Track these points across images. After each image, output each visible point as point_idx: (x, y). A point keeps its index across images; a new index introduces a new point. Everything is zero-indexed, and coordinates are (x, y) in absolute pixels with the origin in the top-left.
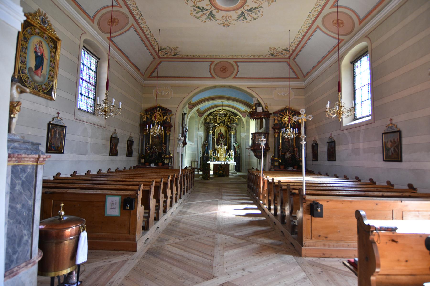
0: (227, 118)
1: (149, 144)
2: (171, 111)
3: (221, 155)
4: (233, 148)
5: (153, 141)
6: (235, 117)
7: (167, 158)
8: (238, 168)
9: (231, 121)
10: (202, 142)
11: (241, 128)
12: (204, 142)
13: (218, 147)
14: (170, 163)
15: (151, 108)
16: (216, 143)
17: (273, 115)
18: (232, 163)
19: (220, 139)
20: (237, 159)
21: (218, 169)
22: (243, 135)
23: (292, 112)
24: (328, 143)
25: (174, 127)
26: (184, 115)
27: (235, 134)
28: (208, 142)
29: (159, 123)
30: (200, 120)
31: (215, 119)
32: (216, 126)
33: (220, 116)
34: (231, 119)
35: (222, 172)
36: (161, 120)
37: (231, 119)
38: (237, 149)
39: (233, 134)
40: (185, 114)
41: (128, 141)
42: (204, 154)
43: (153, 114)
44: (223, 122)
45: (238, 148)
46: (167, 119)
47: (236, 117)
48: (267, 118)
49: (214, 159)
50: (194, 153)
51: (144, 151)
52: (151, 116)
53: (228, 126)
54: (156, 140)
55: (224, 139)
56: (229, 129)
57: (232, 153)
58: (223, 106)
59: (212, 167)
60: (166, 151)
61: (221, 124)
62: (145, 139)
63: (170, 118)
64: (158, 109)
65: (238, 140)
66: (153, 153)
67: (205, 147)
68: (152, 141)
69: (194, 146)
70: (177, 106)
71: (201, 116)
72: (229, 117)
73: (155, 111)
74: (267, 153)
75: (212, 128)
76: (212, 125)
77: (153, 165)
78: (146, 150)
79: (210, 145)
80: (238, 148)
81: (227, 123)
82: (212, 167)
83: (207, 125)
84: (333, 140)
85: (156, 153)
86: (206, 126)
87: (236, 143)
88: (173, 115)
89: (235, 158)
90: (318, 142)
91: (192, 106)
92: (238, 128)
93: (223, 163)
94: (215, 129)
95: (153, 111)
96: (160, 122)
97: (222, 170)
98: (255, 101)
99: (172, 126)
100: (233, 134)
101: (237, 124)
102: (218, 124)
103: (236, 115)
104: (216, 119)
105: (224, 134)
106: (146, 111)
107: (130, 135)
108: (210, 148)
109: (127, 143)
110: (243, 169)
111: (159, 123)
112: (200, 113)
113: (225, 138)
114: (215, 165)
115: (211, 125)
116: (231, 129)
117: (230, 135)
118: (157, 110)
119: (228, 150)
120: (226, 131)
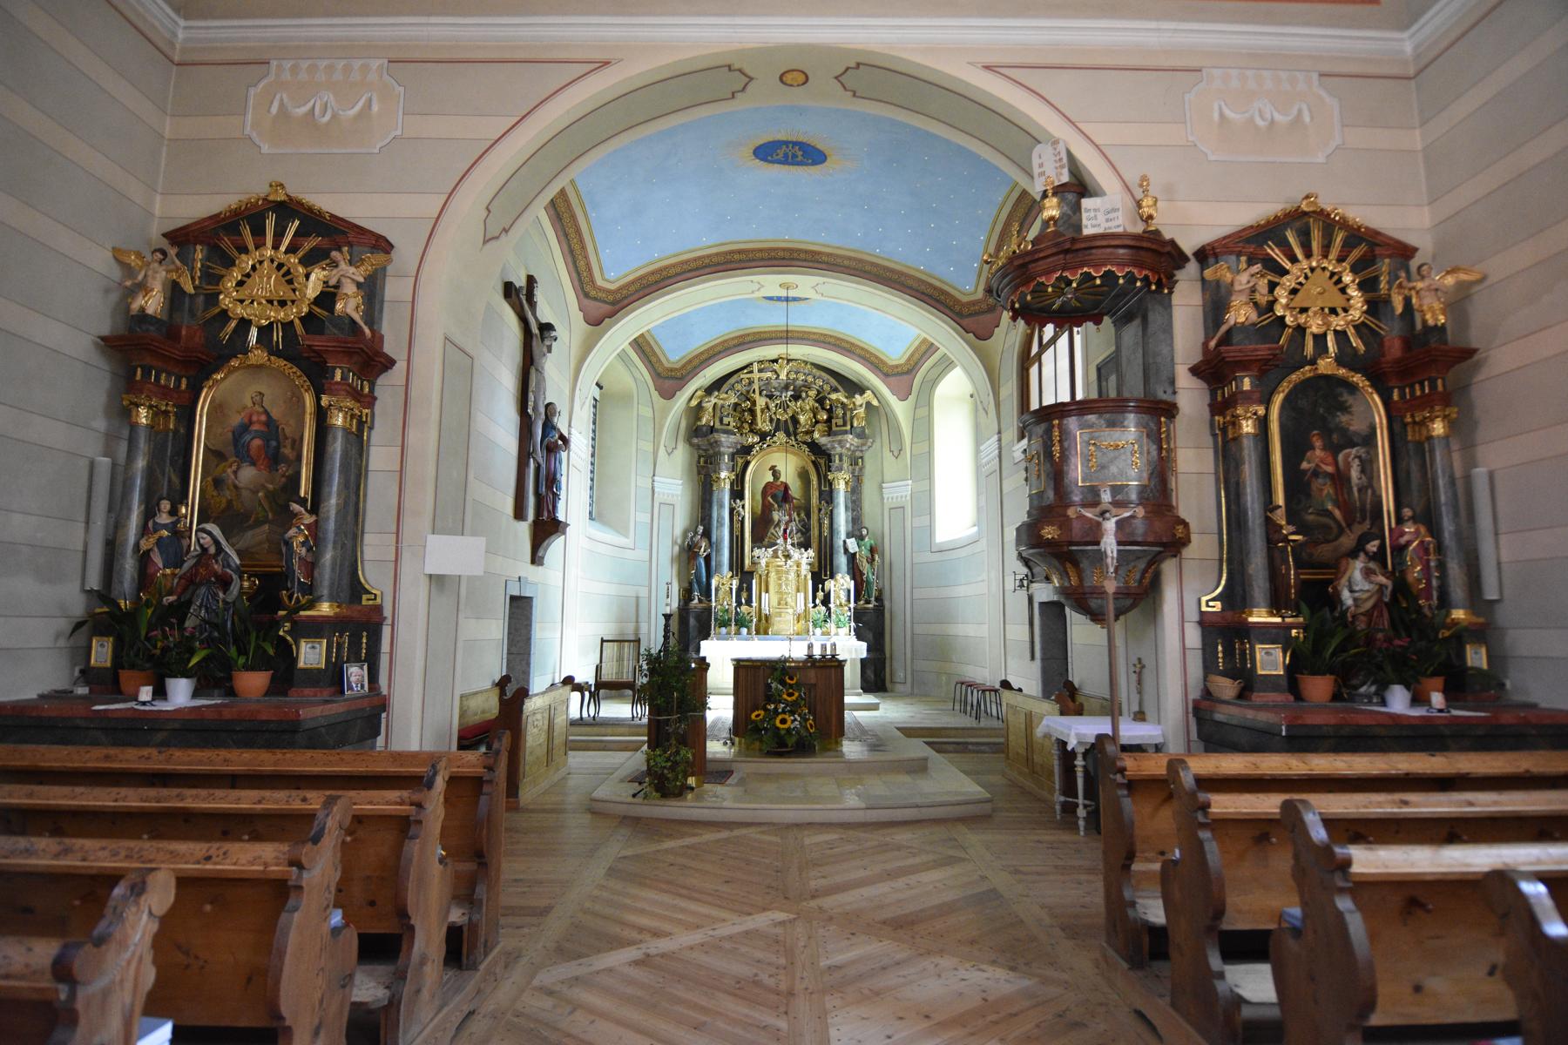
0: (810, 403)
3: (782, 602)
4: (842, 561)
5: (218, 483)
6: (850, 396)
7: (316, 629)
8: (876, 678)
9: (825, 417)
10: (678, 531)
11: (887, 455)
13: (764, 555)
14: (356, 674)
15: (214, 218)
16: (754, 541)
17: (1192, 267)
18: (851, 649)
19: (776, 516)
20: (872, 622)
21: (769, 699)
22: (899, 491)
23: (1348, 246)
25: (401, 366)
26: (536, 337)
28: (707, 534)
29: (277, 336)
31: (745, 413)
32: (751, 447)
33: (770, 397)
34: (830, 411)
35: (793, 722)
36: (292, 313)
37: (830, 411)
38: (865, 568)
39: (841, 487)
40: (546, 328)
42: (687, 595)
43: (230, 263)
44: (790, 427)
45: (871, 561)
46: (327, 298)
47: (859, 399)
48: (1160, 284)
49: (741, 622)
50: (630, 591)
51: (129, 565)
52: (212, 279)
53: (814, 447)
54: (248, 474)
55: (799, 513)
56: (821, 458)
57: (841, 585)
59: (720, 676)
60: (311, 567)
61: (781, 436)
62: (141, 463)
64: (270, 224)
65: (867, 521)
66: (191, 581)
67: (692, 558)
68: (215, 482)
69: (629, 554)
70: (433, 204)
71: (668, 394)
72: (820, 400)
73: (250, 241)
74: (1169, 567)
75: (732, 457)
76: (727, 443)
77: (181, 693)
78: (144, 559)
79: (719, 551)
80: (871, 561)
82: (720, 676)
83: (699, 434)
85: (225, 583)
86: (698, 447)
87: (860, 538)
89: (858, 616)
91: (604, 307)
92: (867, 456)
93: (798, 651)
94: (747, 464)
95: (226, 243)
96: (288, 326)
97: (790, 709)
98: (1050, 169)
99: (390, 363)
101: (861, 435)
102: (763, 436)
103: (854, 387)
104: (752, 412)
105: (795, 490)
106: (181, 238)
108: (719, 565)
110: (900, 675)
111: (277, 336)
112: (669, 380)
113: (798, 509)
114: (744, 669)
115: (723, 438)
116: (829, 458)
117: (828, 496)
118: (259, 232)
119: (822, 572)
120: (804, 476)
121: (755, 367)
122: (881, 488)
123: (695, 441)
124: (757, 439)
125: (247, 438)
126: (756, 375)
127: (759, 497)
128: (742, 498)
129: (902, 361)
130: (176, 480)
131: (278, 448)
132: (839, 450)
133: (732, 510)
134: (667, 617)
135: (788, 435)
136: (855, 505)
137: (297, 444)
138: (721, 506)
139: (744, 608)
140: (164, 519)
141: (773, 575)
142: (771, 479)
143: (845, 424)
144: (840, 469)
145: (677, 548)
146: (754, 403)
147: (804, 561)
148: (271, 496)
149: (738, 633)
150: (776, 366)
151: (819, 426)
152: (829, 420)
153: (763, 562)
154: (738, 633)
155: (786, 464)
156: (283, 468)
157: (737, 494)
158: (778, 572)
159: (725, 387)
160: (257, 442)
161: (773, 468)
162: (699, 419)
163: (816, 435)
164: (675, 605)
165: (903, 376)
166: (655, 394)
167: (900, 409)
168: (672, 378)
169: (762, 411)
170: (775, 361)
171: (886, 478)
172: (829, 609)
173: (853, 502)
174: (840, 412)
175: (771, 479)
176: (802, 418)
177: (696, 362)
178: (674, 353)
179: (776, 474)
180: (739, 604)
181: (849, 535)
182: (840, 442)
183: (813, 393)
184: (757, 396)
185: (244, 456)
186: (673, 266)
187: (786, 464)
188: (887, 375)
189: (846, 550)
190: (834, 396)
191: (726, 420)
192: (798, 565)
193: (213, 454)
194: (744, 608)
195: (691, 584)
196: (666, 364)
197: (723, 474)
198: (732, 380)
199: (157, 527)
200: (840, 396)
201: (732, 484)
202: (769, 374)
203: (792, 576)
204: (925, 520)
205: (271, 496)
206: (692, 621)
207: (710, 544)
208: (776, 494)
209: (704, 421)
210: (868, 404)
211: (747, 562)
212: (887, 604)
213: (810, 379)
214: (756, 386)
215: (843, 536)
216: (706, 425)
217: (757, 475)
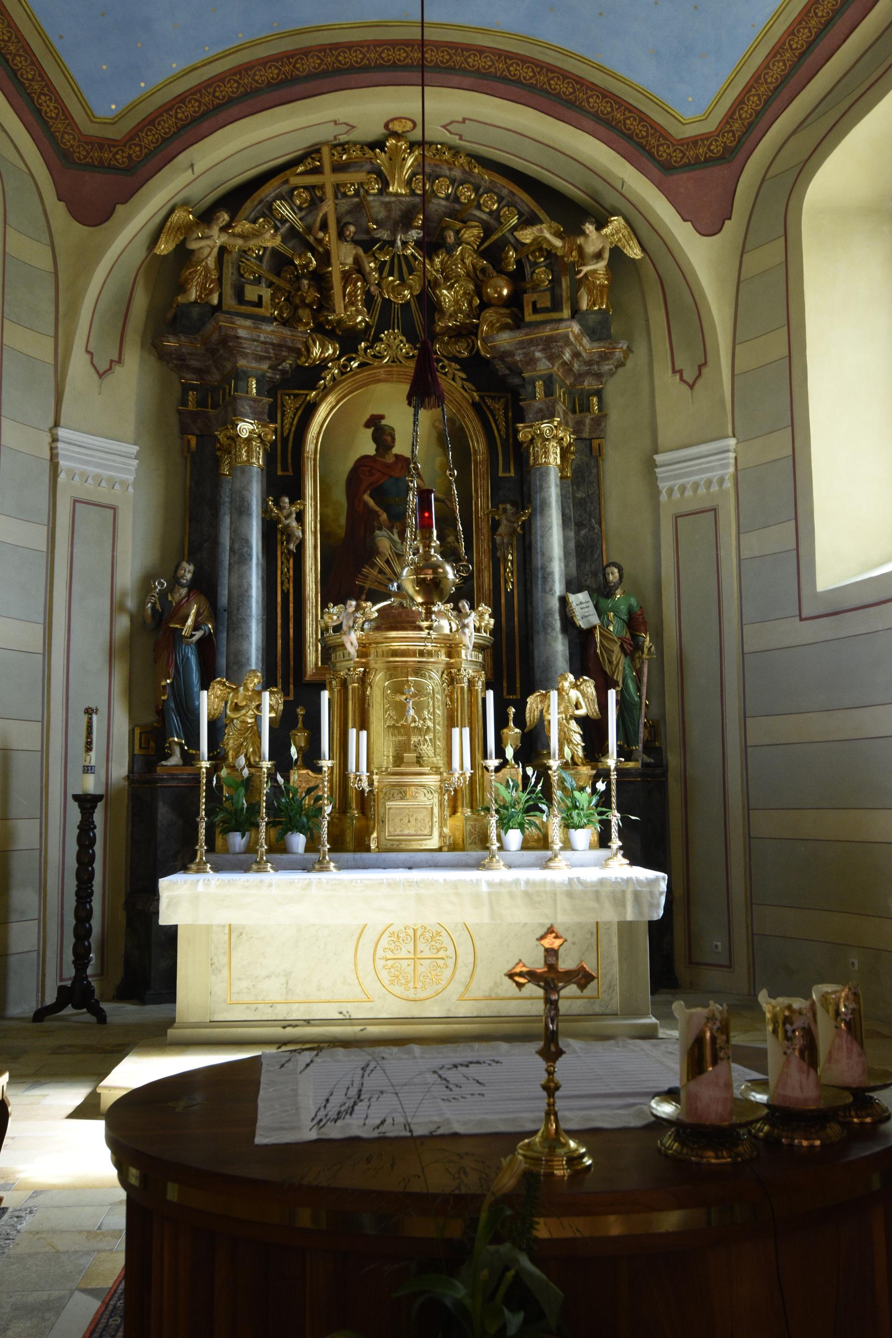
10: (128, 576)
12: (146, 583)
13: (353, 625)
22: (703, 466)
27: (584, 477)
28: (205, 585)
30: (86, 260)
31: (298, 281)
32: (322, 366)
33: (367, 244)
34: (518, 278)
37: (518, 278)
45: (632, 649)
47: (593, 239)
49: (289, 816)
72: (492, 253)
75: (270, 388)
76: (255, 338)
80: (632, 649)
87: (602, 593)
92: (613, 389)
94: (311, 409)
100: (554, 459)
102: (349, 339)
103: (573, 212)
104: (320, 280)
119: (513, 669)
121: (325, 150)
122: (651, 466)
123: (171, 343)
126: (328, 179)
127: (340, 494)
128: (297, 494)
129: (711, 125)
132: (544, 366)
134: (87, 803)
136: (585, 513)
138: (242, 510)
139: (299, 777)
141: (379, 680)
142: (369, 448)
143: (556, 306)
145: (123, 623)
146: (325, 258)
147: (469, 638)
149: (279, 847)
150: (381, 159)
151: (489, 314)
152: (514, 302)
153: (352, 640)
154: (279, 847)
157: (284, 482)
158: (393, 671)
159: (249, 206)
161: (375, 422)
162: (182, 288)
164: (120, 770)
166: (58, 211)
167: (702, 256)
170: (378, 144)
171: (665, 437)
172: (543, 772)
173: (580, 504)
174: (543, 275)
175: (369, 448)
176: (446, 295)
177: (168, 124)
180: (282, 762)
181: (572, 586)
183: (472, 234)
184: (330, 238)
188: (667, 167)
190: (527, 236)
191: (251, 293)
192: (452, 650)
194: (299, 777)
195: (161, 713)
197: (245, 428)
198: (268, 191)
200: (546, 232)
201: (270, 458)
202: (361, 176)
203: (434, 681)
204: (780, 537)
207: (213, 611)
208: (376, 486)
209: (193, 295)
210: (617, 253)
211: (312, 657)
212: (673, 760)
213: (467, 194)
214: (328, 208)
215: (558, 588)
216: (202, 304)
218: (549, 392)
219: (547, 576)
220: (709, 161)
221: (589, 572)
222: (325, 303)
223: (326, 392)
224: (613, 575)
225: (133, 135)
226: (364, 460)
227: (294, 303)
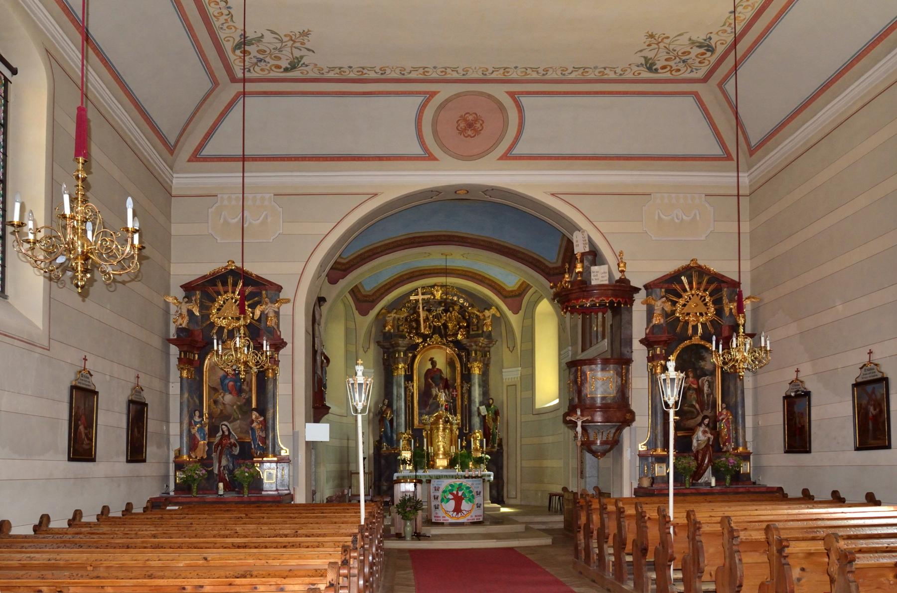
0: (455, 314)
1: (201, 416)
2: (279, 288)
4: (476, 421)
5: (216, 402)
12: (376, 404)
15: (204, 277)
22: (512, 374)
24: (856, 385)
25: (289, 346)
27: (485, 374)
28: (390, 405)
31: (413, 323)
32: (418, 344)
33: (429, 311)
39: (476, 372)
41: (130, 402)
44: (441, 331)
47: (487, 313)
53: (457, 344)
54: (228, 398)
58: (446, 272)
63: (277, 314)
65: (493, 394)
71: (364, 313)
75: (405, 354)
79: (398, 416)
80: (495, 420)
81: (456, 334)
84: (879, 376)
87: (488, 406)
88: (287, 301)
90: (809, 386)
94: (414, 357)
99: (286, 344)
102: (425, 337)
105: (446, 372)
107: (133, 379)
108: (398, 425)
109: (125, 411)
115: (401, 341)
116: (468, 354)
117: (467, 377)
120: (451, 363)
122: (501, 372)
124: (420, 340)
125: (227, 381)
127: (423, 380)
128: (412, 381)
130: (197, 401)
131: (241, 386)
132: (474, 347)
133: (406, 388)
135: (441, 337)
137: (249, 384)
138: (399, 386)
140: (197, 419)
142: (429, 366)
144: (476, 360)
146: (419, 316)
148: (239, 407)
152: (468, 326)
155: (440, 356)
156: (243, 395)
160: (231, 383)
161: (431, 359)
163: (459, 337)
165: (515, 298)
166: (356, 313)
167: (514, 319)
168: (366, 301)
169: (424, 322)
170: (433, 286)
171: (505, 365)
175: (429, 366)
177: (383, 291)
178: (369, 287)
179: (434, 363)
182: (475, 342)
183: (457, 308)
185: (226, 389)
186: (380, 247)
187: (440, 356)
188: (505, 297)
189: (479, 414)
191: (401, 328)
193: (213, 390)
195: (381, 437)
196: (364, 293)
199: (196, 423)
205: (239, 407)
206: (383, 462)
207: (392, 412)
208: (433, 376)
209: (387, 329)
211: (416, 422)
215: (477, 405)
217: (421, 365)
218: (476, 354)
219: (475, 402)
220: (516, 296)
221: (486, 400)
222: (418, 327)
223: (419, 352)
224: (491, 401)
225: (374, 294)
226: (429, 370)
227: (411, 327)
